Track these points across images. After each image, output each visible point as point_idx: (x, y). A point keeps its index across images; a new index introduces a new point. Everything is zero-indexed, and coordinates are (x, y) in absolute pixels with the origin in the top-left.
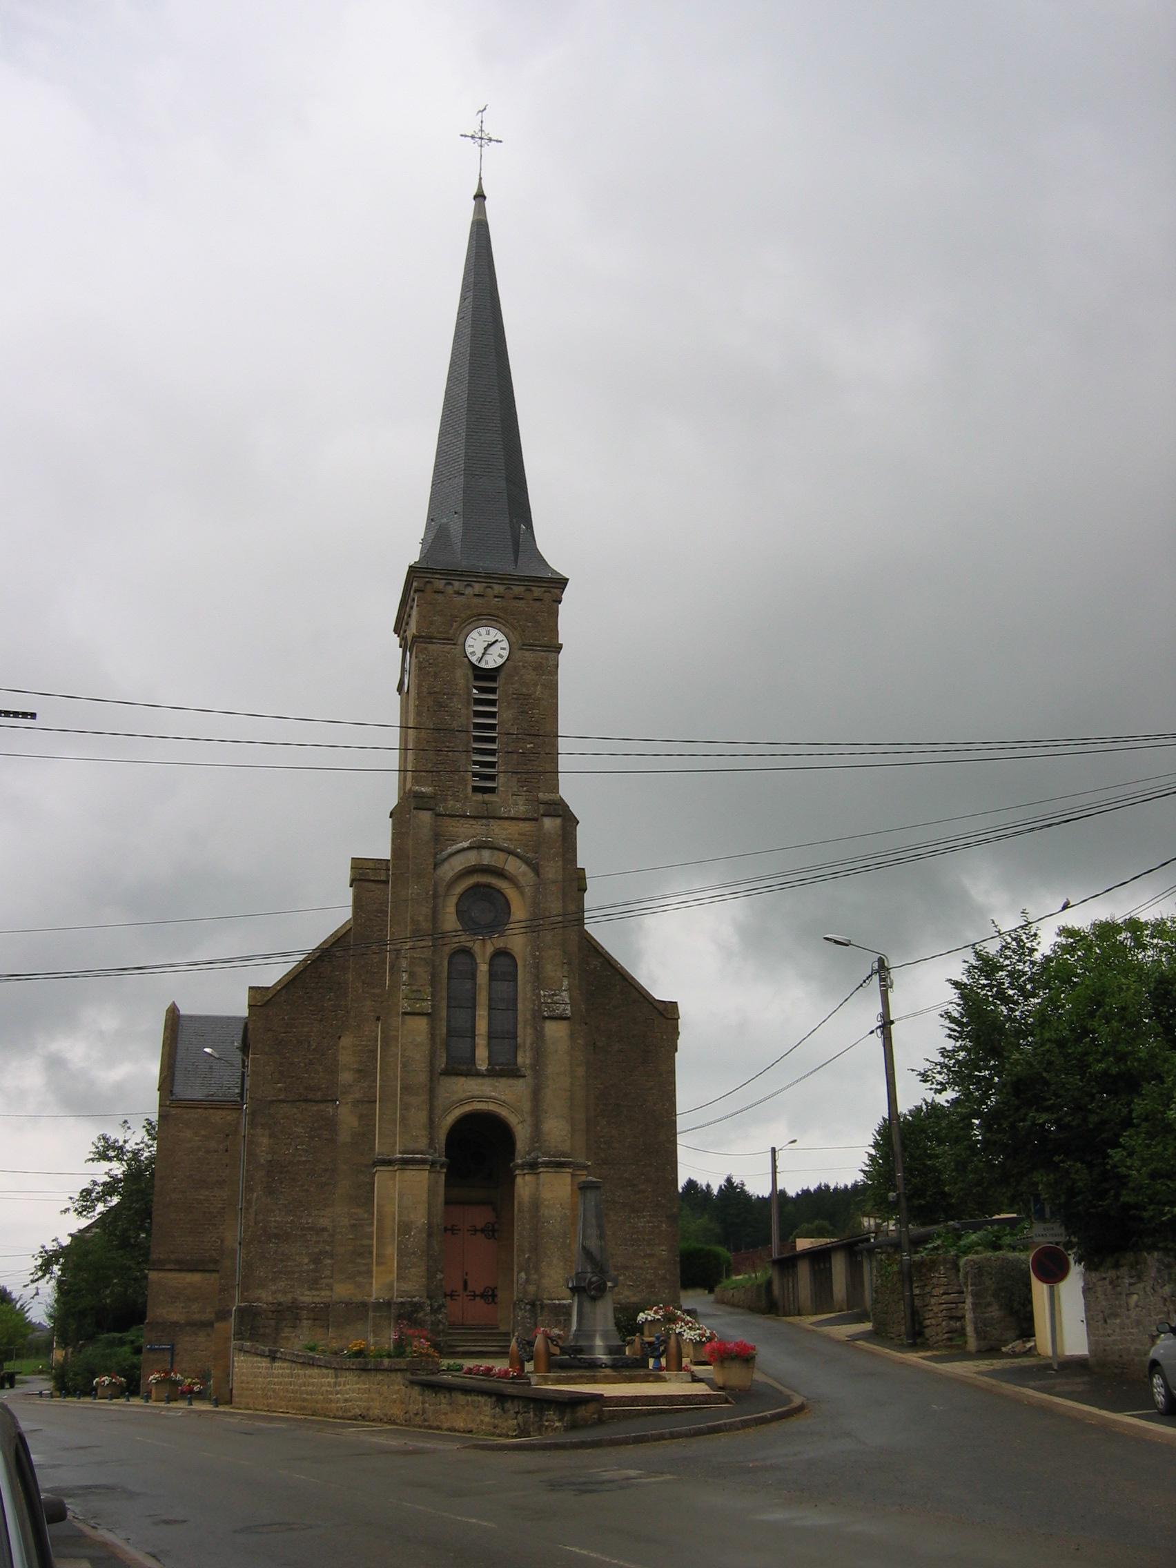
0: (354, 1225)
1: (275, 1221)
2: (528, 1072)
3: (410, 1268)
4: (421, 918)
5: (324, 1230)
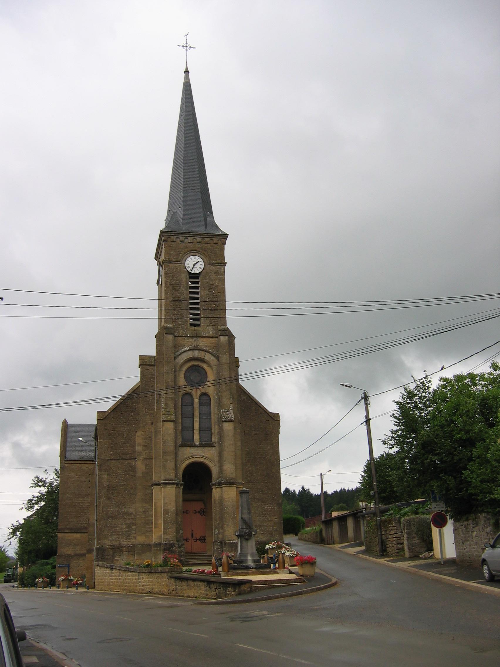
0: (144, 512)
1: (111, 511)
2: (217, 445)
3: (169, 529)
4: (169, 380)
5: (132, 513)
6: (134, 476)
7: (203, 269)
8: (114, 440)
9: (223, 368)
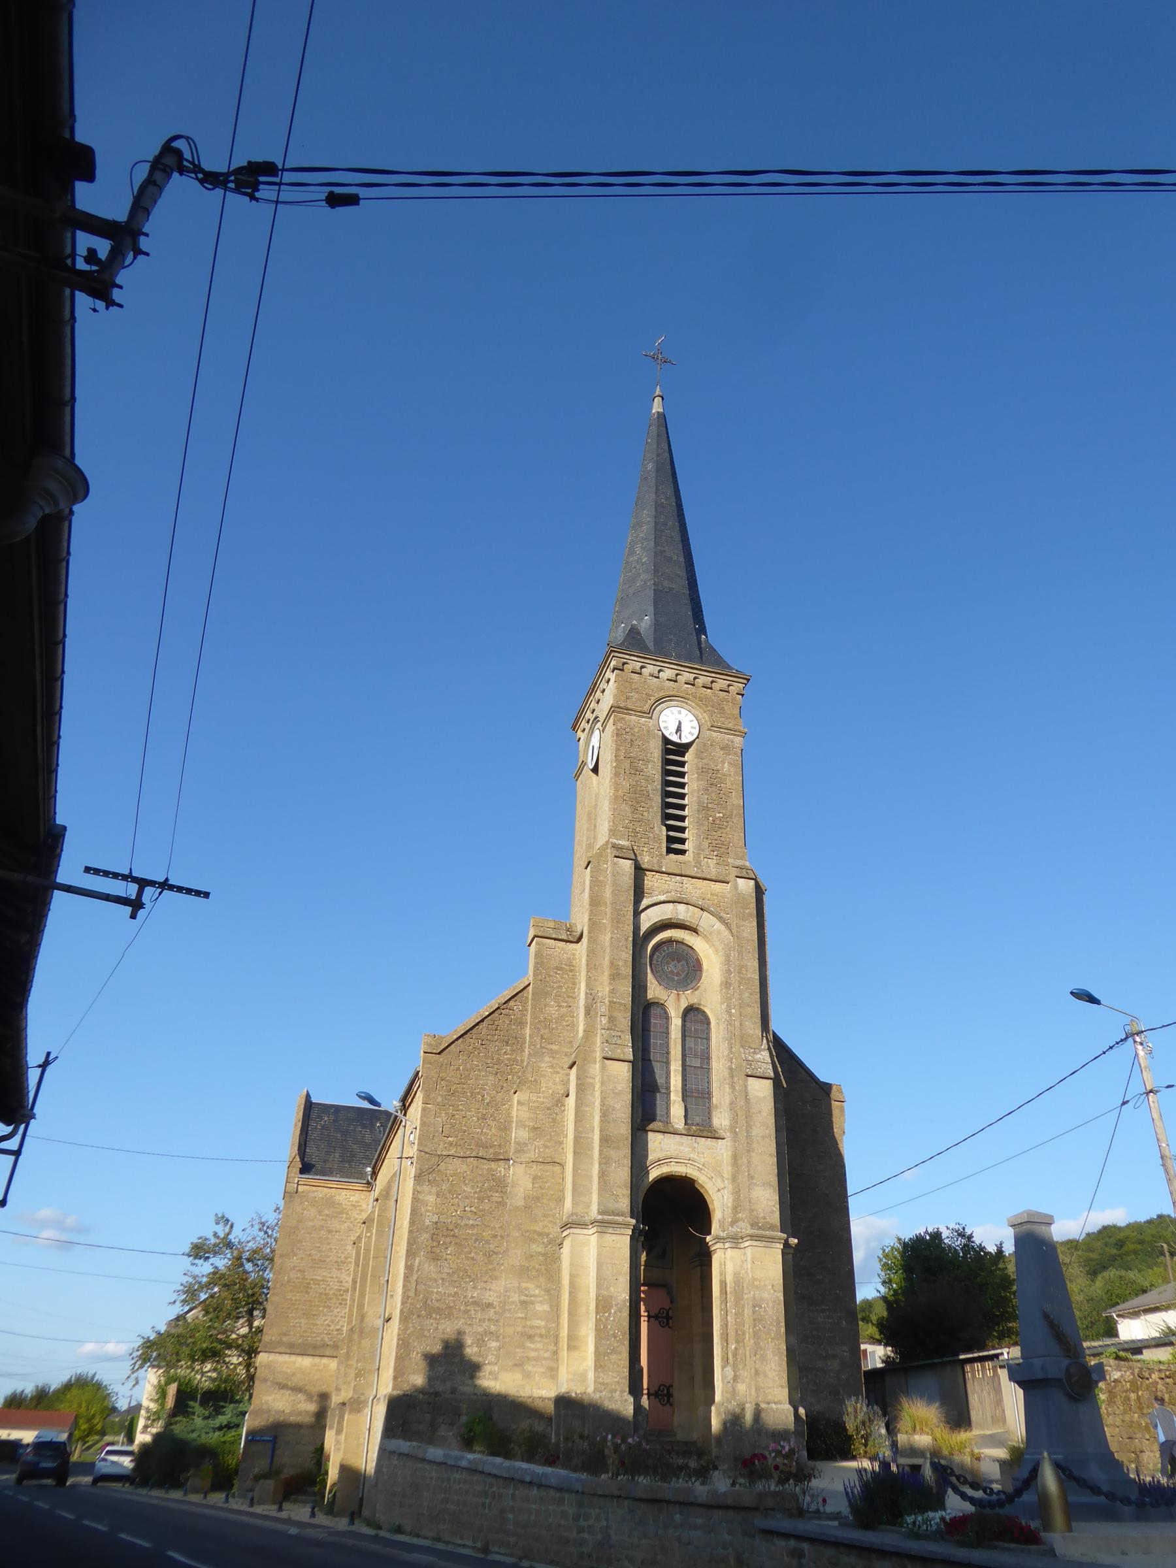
0: (523, 1303)
1: (437, 1293)
2: (727, 1135)
3: (611, 1353)
4: (621, 963)
5: (490, 1305)
6: (502, 1204)
7: (697, 737)
8: (461, 1107)
9: (744, 949)
